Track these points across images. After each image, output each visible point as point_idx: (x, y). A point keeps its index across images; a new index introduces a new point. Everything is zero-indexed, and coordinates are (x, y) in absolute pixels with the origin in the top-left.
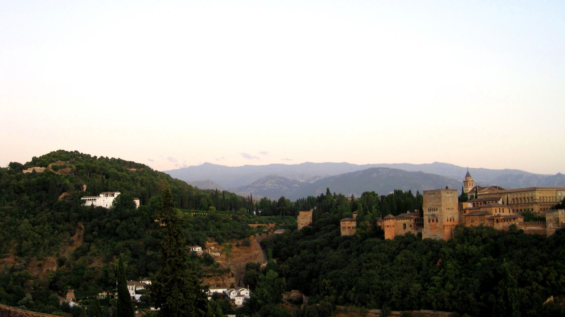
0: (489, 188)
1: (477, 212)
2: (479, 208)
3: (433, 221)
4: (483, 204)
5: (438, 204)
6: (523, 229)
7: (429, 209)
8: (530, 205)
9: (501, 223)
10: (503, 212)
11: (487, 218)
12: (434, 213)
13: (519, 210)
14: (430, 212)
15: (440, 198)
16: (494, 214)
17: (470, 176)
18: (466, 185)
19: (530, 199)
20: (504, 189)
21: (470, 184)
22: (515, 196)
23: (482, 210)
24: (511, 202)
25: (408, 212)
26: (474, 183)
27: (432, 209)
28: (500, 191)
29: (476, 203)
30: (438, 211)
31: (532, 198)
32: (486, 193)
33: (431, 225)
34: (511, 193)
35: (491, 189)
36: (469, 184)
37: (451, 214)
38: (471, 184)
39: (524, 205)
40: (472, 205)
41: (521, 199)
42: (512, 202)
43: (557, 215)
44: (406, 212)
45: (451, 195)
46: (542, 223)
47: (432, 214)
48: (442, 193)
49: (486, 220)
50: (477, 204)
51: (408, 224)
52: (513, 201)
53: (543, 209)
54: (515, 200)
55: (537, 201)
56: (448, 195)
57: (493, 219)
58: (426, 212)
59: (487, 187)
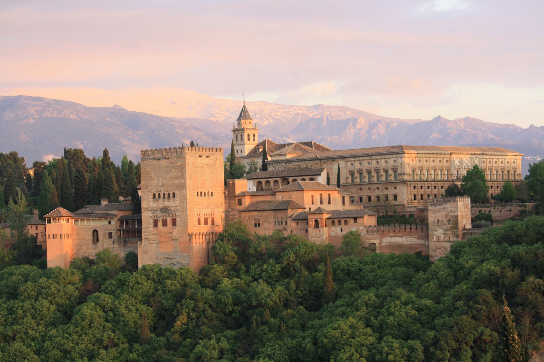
0: (295, 147)
2: (274, 194)
3: (165, 223)
4: (280, 184)
5: (176, 182)
6: (377, 242)
7: (154, 195)
8: (389, 188)
9: (325, 228)
10: (329, 203)
11: (291, 217)
12: (166, 203)
13: (365, 199)
15: (182, 168)
16: (308, 204)
17: (250, 119)
18: (239, 137)
19: (391, 172)
20: (327, 150)
21: (248, 135)
22: (357, 165)
24: (347, 178)
25: (104, 203)
26: (259, 136)
28: (319, 155)
29: (263, 181)
30: (176, 199)
31: (395, 170)
32: (289, 157)
33: (159, 234)
34: (347, 160)
35: (301, 149)
37: (208, 207)
38: (251, 137)
39: (376, 186)
40: (254, 185)
41: (369, 173)
42: (350, 181)
43: (453, 209)
44: (99, 203)
45: (207, 160)
46: (419, 230)
47: (161, 206)
48: (187, 156)
49: (289, 221)
50: (268, 182)
53: (420, 197)
54: (357, 175)
55: (406, 177)
56: (200, 159)
57: (306, 220)
58: (147, 202)
59: (289, 145)
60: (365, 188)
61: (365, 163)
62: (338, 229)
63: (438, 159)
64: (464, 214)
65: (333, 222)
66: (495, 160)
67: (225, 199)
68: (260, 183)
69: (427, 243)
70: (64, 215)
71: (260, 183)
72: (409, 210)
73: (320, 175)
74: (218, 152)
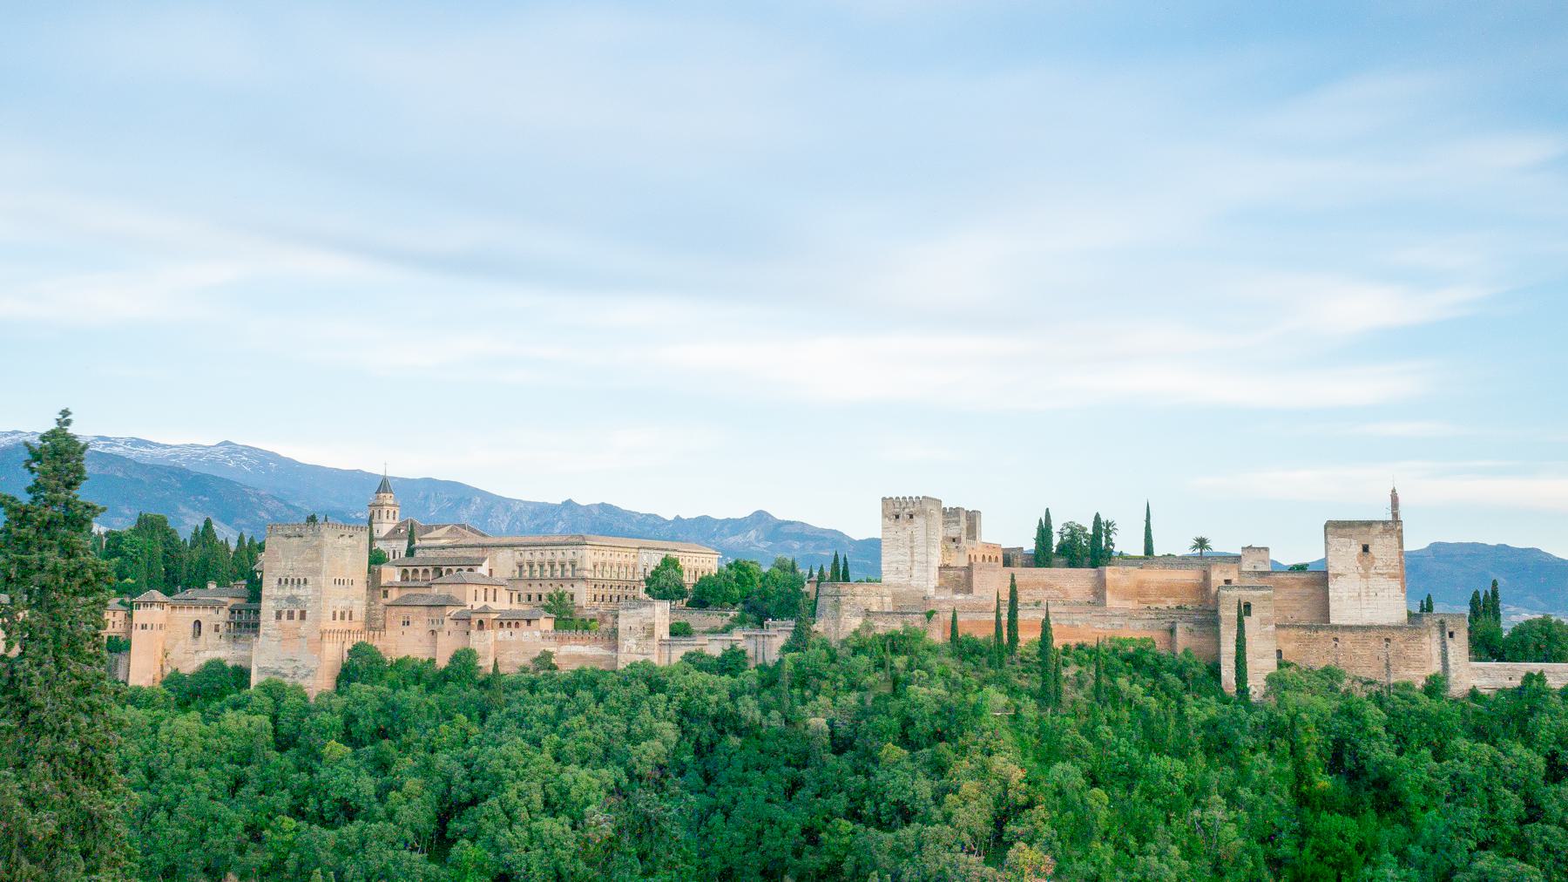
0: (451, 529)
1: (422, 595)
2: (429, 586)
4: (431, 573)
5: (310, 565)
7: (280, 580)
10: (495, 600)
12: (295, 592)
14: (283, 588)
19: (568, 567)
22: (527, 556)
23: (435, 590)
25: (212, 586)
27: (290, 581)
29: (410, 570)
32: (442, 542)
33: (282, 629)
34: (515, 548)
36: (385, 514)
42: (517, 574)
44: (204, 586)
47: (289, 594)
48: (326, 535)
50: (415, 571)
51: (206, 624)
52: (517, 569)
54: (526, 567)
57: (469, 620)
58: (270, 589)
60: (535, 584)
61: (538, 554)
62: (507, 632)
63: (625, 554)
64: (661, 621)
65: (501, 624)
66: (688, 558)
67: (367, 590)
68: (405, 571)
69: (614, 655)
70: (159, 600)
71: (405, 571)
72: (588, 613)
73: (481, 565)
74: (364, 532)
